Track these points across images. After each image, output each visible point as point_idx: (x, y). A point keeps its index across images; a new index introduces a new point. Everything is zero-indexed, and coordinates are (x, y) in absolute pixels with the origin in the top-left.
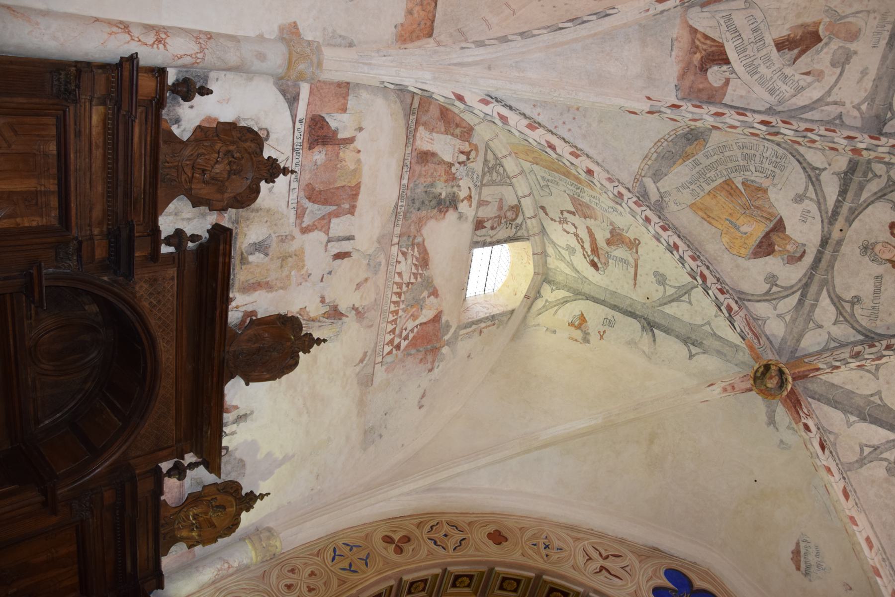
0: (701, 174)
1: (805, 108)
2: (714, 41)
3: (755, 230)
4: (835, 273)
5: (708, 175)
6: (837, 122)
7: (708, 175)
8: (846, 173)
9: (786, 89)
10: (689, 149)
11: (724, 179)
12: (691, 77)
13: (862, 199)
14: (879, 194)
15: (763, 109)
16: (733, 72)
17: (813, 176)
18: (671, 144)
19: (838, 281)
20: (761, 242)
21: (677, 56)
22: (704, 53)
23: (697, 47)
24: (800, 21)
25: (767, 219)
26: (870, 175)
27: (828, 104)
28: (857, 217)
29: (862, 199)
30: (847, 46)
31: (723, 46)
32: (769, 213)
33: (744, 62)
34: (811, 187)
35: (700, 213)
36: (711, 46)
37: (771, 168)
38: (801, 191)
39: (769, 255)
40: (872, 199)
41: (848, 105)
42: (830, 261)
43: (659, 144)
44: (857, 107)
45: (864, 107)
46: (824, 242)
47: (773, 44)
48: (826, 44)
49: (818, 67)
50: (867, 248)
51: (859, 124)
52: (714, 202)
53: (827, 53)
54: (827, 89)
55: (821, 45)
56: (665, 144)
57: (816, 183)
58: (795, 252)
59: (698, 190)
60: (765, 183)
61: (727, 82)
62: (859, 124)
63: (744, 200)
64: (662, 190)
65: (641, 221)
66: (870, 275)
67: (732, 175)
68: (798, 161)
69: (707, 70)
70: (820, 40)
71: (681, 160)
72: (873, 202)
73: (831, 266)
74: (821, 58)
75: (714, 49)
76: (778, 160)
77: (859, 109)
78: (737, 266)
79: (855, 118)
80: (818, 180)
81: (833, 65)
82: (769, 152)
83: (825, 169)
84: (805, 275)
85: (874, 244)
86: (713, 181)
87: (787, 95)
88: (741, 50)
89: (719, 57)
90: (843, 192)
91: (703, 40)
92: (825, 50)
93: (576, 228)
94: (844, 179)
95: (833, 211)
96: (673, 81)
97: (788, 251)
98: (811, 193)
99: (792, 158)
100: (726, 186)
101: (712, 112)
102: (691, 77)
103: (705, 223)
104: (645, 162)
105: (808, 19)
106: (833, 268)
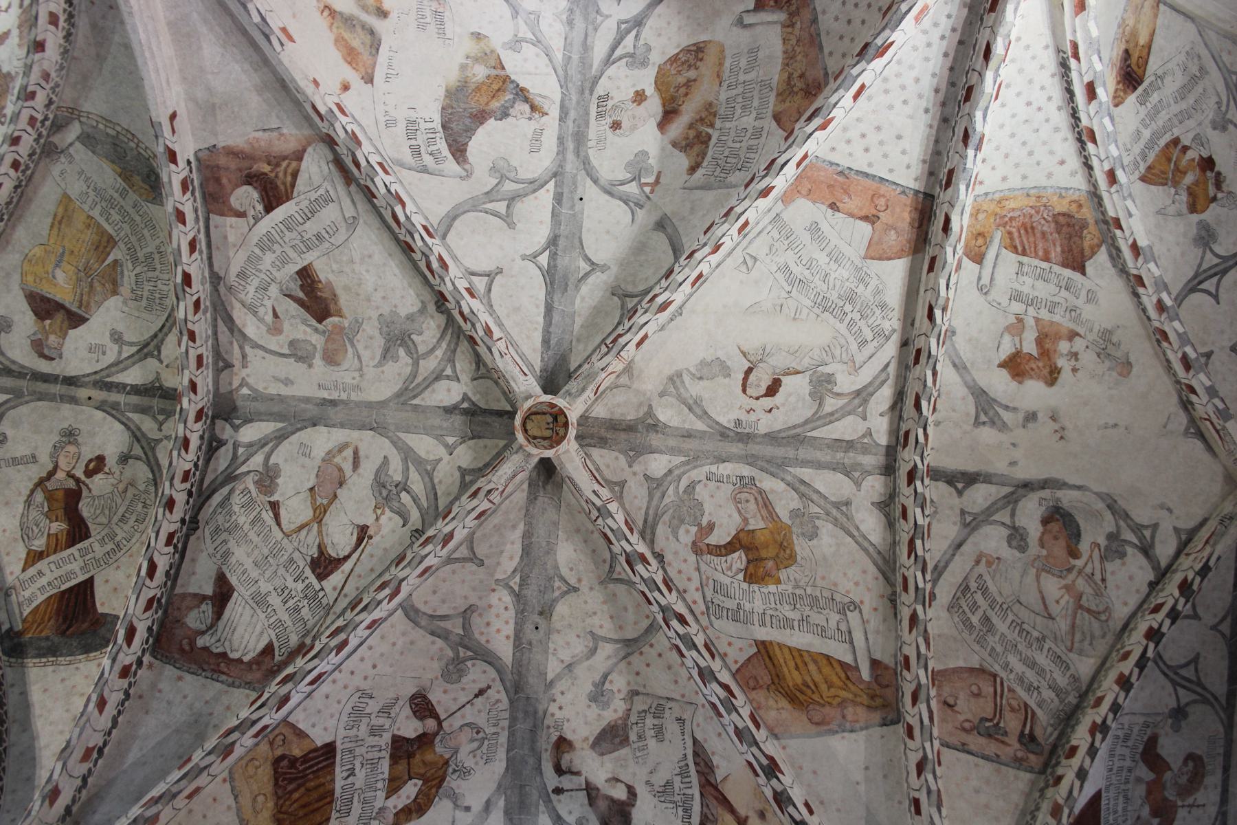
0: (111, 202)
1: (229, 321)
2: (293, 185)
3: (62, 287)
4: (32, 405)
5: (112, 212)
6: (221, 364)
7: (112, 212)
8: (161, 387)
9: (250, 292)
10: (137, 179)
11: (114, 234)
12: (233, 164)
13: (130, 415)
14: (138, 434)
15: (216, 269)
16: (257, 220)
17: (149, 349)
18: (135, 152)
19: (24, 409)
20: (49, 300)
21: (258, 140)
22: (273, 175)
23: (278, 165)
24: (339, 292)
25: (81, 302)
26: (161, 418)
27: (241, 348)
28: (109, 414)
29: (130, 415)
30: (318, 356)
31: (288, 199)
32: (88, 303)
33: (273, 231)
34: (135, 349)
35: (61, 210)
36: (284, 184)
37: (146, 294)
38: (126, 338)
39: (36, 315)
40: (132, 427)
41: (244, 373)
42: (47, 394)
43: (129, 136)
44: (243, 383)
45: (245, 391)
46: (71, 381)
47: (305, 263)
48: (316, 330)
49: (286, 326)
50: (70, 436)
51: (222, 390)
52: (80, 226)
53: (305, 332)
54: (260, 343)
55: (314, 322)
56: (132, 145)
57: (142, 355)
58: (50, 348)
59: (90, 201)
60: (125, 289)
61: (242, 215)
62: (222, 390)
63: (96, 266)
64: (71, 150)
65: (10, 132)
66: (36, 448)
67: (121, 244)
68: (163, 326)
69: (250, 184)
70: (320, 321)
71: (119, 170)
72: (128, 428)
73: (41, 397)
74: (299, 326)
75: (282, 187)
76: (157, 301)
77: (241, 385)
78: (8, 275)
79: (230, 384)
80: (146, 357)
81: (292, 344)
82: (165, 288)
83: (161, 362)
84: (23, 367)
85: (76, 443)
86: (107, 220)
87: (242, 296)
88: (288, 224)
89: (273, 197)
90: (136, 390)
91: (290, 171)
92: (308, 330)
93: (6, 11)
94: (153, 387)
95: (111, 383)
96: (222, 141)
97: (47, 338)
98: (128, 351)
99: (164, 318)
100: (105, 239)
101: (181, 207)
102: (233, 164)
103: (50, 220)
104: (100, 119)
105: (344, 301)
106: (39, 400)
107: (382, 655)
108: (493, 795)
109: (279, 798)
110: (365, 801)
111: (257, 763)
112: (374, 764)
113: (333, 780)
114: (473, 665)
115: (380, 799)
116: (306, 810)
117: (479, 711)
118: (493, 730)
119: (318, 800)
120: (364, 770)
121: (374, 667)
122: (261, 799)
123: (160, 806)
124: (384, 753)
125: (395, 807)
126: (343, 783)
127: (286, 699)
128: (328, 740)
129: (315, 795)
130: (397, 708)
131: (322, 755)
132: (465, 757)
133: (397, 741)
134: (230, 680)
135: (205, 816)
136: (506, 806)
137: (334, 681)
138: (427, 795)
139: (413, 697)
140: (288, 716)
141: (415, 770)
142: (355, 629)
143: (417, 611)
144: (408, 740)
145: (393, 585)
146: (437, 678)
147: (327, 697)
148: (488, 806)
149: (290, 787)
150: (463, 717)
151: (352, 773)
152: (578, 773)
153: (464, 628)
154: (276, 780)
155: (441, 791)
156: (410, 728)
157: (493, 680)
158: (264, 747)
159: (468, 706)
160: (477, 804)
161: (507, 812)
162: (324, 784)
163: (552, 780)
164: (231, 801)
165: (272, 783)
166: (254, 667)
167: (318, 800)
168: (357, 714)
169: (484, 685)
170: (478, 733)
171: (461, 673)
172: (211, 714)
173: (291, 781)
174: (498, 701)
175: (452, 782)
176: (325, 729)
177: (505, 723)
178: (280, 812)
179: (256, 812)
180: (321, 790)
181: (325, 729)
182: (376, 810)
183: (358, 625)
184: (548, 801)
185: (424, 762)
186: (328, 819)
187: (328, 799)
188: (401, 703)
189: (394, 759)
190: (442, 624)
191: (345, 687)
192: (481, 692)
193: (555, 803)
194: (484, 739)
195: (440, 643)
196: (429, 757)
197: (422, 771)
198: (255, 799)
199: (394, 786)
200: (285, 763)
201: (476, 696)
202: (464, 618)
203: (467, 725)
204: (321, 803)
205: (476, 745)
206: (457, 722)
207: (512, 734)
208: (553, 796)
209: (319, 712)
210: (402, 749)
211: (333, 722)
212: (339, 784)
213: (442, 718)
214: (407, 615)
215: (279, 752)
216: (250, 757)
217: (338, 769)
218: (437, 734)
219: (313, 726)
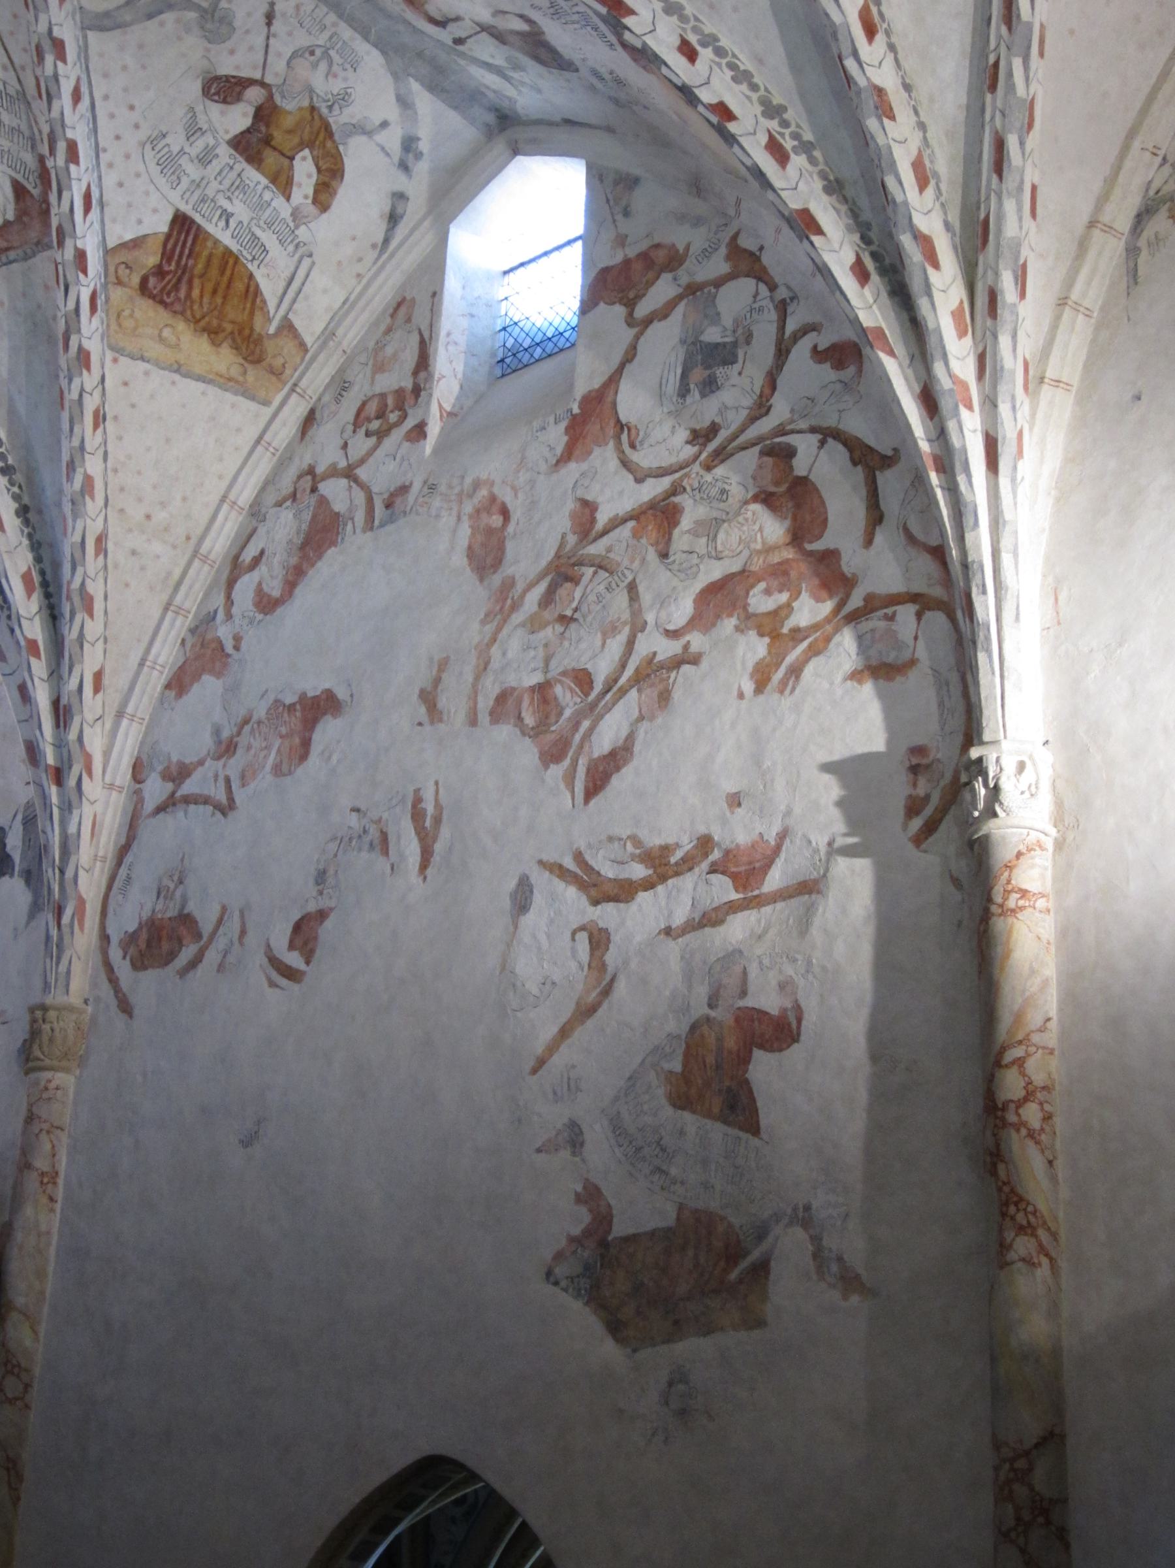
107: (125, 90)
109: (182, 313)
110: (269, 225)
111: (127, 313)
112: (240, 186)
113: (217, 242)
116: (220, 292)
118: (326, 35)
119: (222, 273)
120: (236, 202)
121: (132, 108)
122: (166, 333)
123: (80, 471)
124: (238, 167)
125: (306, 197)
126: (228, 233)
127: (81, 256)
128: (169, 217)
129: (214, 272)
131: (179, 233)
134: (20, 252)
135: (133, 406)
136: (423, 84)
137: (110, 165)
138: (327, 154)
139: (206, 91)
142: (63, 126)
143: (107, 14)
144: (248, 131)
145: (47, 45)
148: (404, 103)
150: (279, 55)
151: (227, 216)
152: (457, 19)
154: (162, 302)
155: (336, 137)
156: (239, 118)
159: (272, 41)
160: (387, 109)
161: (433, 88)
162: (210, 256)
163: (445, 36)
164: (142, 366)
165: (161, 309)
166: (25, 219)
168: (169, 165)
169: (264, 8)
170: (312, 53)
172: (39, 307)
173: (176, 287)
175: (337, 120)
176: (155, 211)
177: (332, 17)
178: (197, 322)
180: (216, 262)
181: (155, 211)
182: (290, 220)
183: (63, 120)
184: (462, 55)
185: (290, 132)
186: (251, 276)
187: (231, 261)
188: (199, 108)
189: (254, 159)
191: (127, 156)
192: (270, 18)
196: (288, 122)
197: (296, 140)
198: (161, 339)
199: (283, 182)
200: (152, 281)
201: (269, 24)
203: (295, 55)
204: (228, 272)
205: (323, 66)
207: (351, 21)
208: (460, 48)
209: (130, 205)
210: (252, 146)
212: (226, 239)
213: (257, 75)
214: (102, 29)
215: (136, 280)
217: (210, 228)
218: (271, 97)
219: (140, 222)
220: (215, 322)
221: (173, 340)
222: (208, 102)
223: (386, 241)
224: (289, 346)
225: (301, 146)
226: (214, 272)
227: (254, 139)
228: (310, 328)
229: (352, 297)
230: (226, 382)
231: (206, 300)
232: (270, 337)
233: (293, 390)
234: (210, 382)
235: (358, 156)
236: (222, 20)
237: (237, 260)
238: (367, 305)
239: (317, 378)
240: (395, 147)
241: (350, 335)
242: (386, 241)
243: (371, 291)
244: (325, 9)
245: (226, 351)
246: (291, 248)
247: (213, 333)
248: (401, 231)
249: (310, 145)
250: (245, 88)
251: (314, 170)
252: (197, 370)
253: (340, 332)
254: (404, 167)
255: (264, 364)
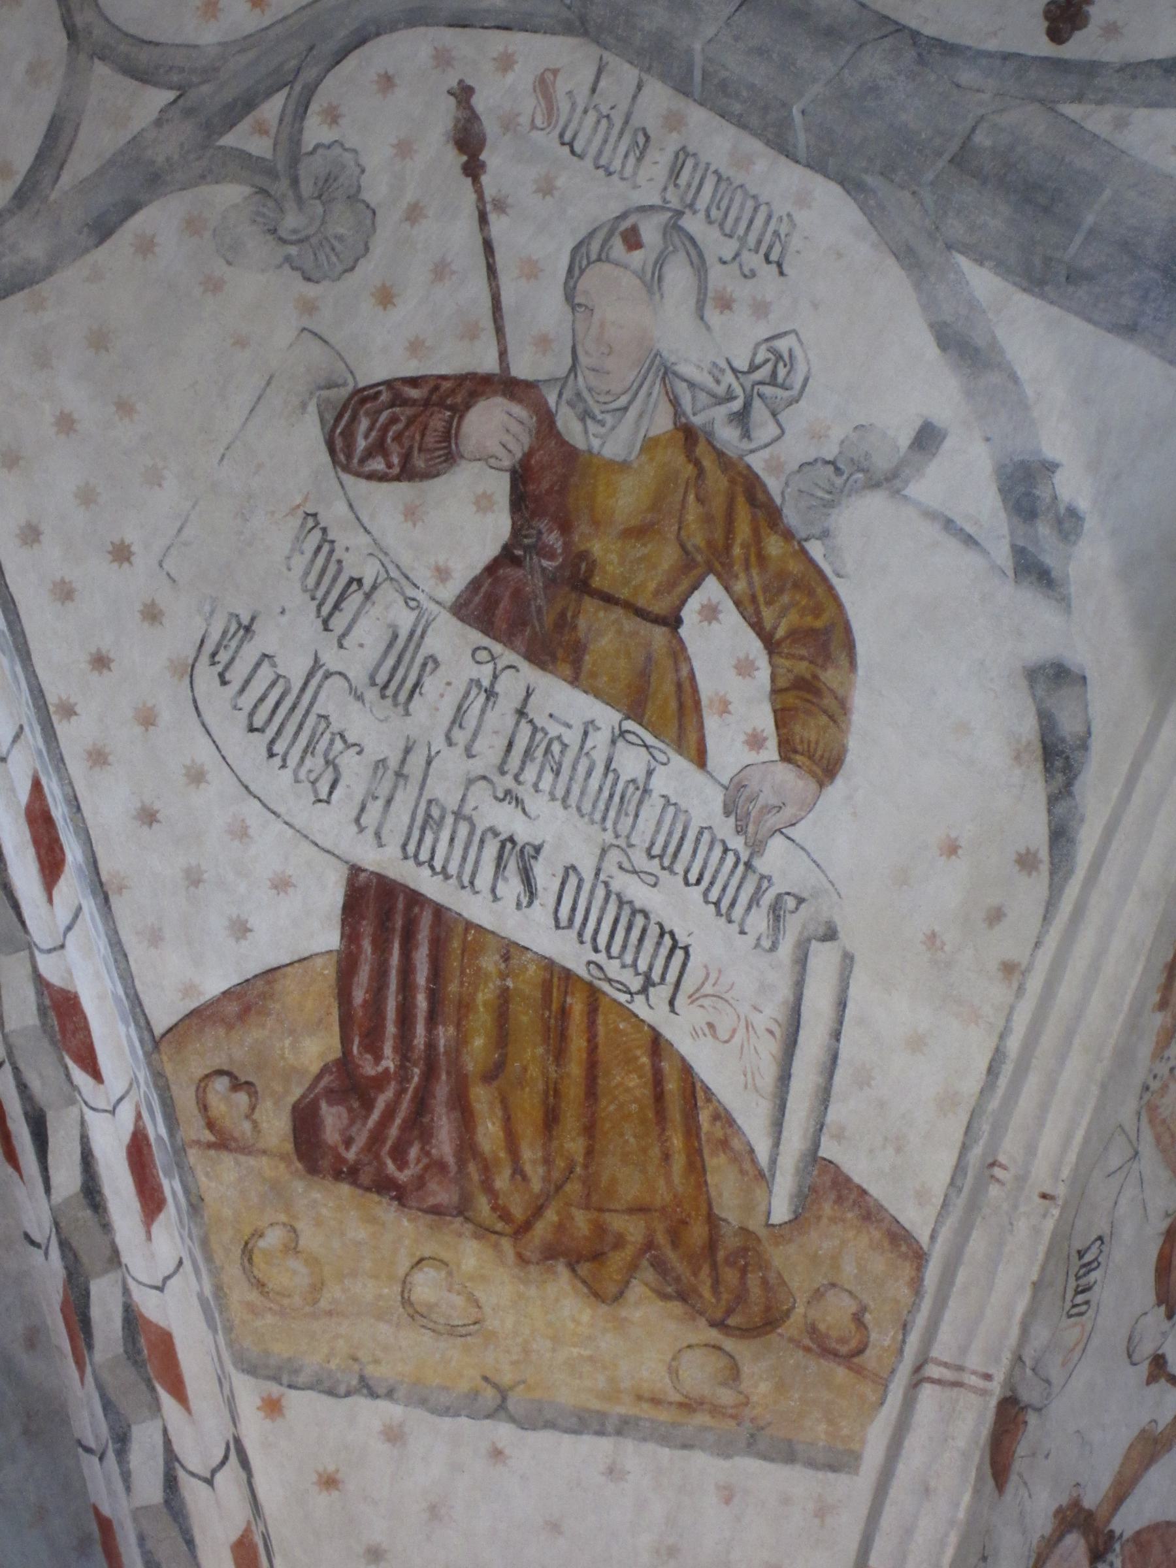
108: (929, 305)
109: (463, 1209)
110: (665, 857)
111: (273, 1238)
112: (530, 747)
113: (510, 950)
114: (332, 116)
115: (696, 795)
116: (571, 1121)
117: (546, 188)
118: (659, 162)
119: (559, 1054)
120: (537, 804)
121: (122, 554)
124: (510, 687)
125: (755, 742)
126: (541, 912)
128: (333, 896)
129: (531, 1054)
130: (350, 541)
131: (381, 947)
132: (706, 348)
133: (493, 604)
136: (1002, 268)
137: (98, 757)
138: (779, 583)
139: (340, 449)
140: (143, 1023)
141: (646, 587)
144: (508, 557)
146: (309, 307)
147: (149, 817)
148: (965, 347)
149: (444, 1143)
150: (532, 270)
151: (520, 858)
153: (144, 76)
154: (384, 1186)
155: (791, 517)
156: (461, 522)
157: (443, 59)
158: (224, 1180)
159: (498, 226)
161: (1040, 276)
162: (505, 996)
164: (374, 1414)
165: (385, 1209)
167: (556, 1038)
168: (286, 721)
169: (445, 115)
170: (633, 240)
171: (339, 188)
173: (418, 1124)
174: (544, 85)
175: (778, 453)
176: (281, 885)
177: (658, 98)
178: (526, 1227)
179: (471, 1329)
180: (524, 1017)
181: (281, 885)
182: (725, 828)
185: (639, 532)
186: (657, 1044)
187: (577, 1006)
188: (335, 512)
189: (554, 648)
190: (81, 164)
191: (147, 719)
192: (469, 143)
193: (1113, 52)
194: (673, 228)
195: (160, 218)
196: (626, 500)
197: (669, 556)
198: (415, 1313)
199: (667, 707)
200: (332, 1120)
201: (473, 169)
202: (102, 54)
203: (573, 272)
204: (578, 1043)
205: (678, 276)
206: (539, 309)
207: (717, 94)
208: (1078, 47)
209: (194, 878)
210: (533, 602)
211: (269, 839)
212: (539, 934)
213: (488, 363)
215: (276, 1126)
216: (237, 1260)
217: (474, 908)
218: (546, 421)
219: (241, 929)
220: (581, 1221)
221: (454, 1307)
222: (359, 487)
223: (1061, 836)
224: (856, 1255)
225: (690, 571)
226: (531, 1054)
227: (530, 579)
228: (909, 1178)
229: (1013, 1045)
230: (676, 1418)
231: (529, 1154)
232: (780, 1233)
233: (918, 1379)
234: (624, 1427)
235: (877, 563)
236: (326, 185)
237: (593, 995)
238: (1068, 1036)
239: (984, 1310)
240: (984, 507)
241: (1049, 1141)
242: (1061, 836)
243: (1066, 994)
244: (630, 74)
245: (644, 1308)
246: (759, 921)
247: (586, 1259)
248: (1095, 795)
249: (716, 560)
250: (460, 411)
251: (755, 647)
252: (569, 1393)
253: (1010, 1148)
254: (1032, 570)
255: (793, 1326)
